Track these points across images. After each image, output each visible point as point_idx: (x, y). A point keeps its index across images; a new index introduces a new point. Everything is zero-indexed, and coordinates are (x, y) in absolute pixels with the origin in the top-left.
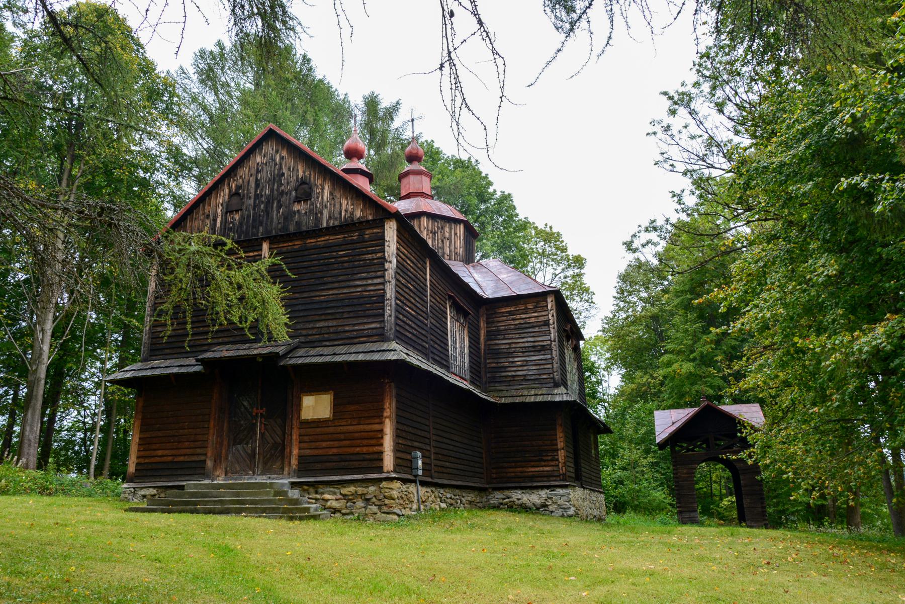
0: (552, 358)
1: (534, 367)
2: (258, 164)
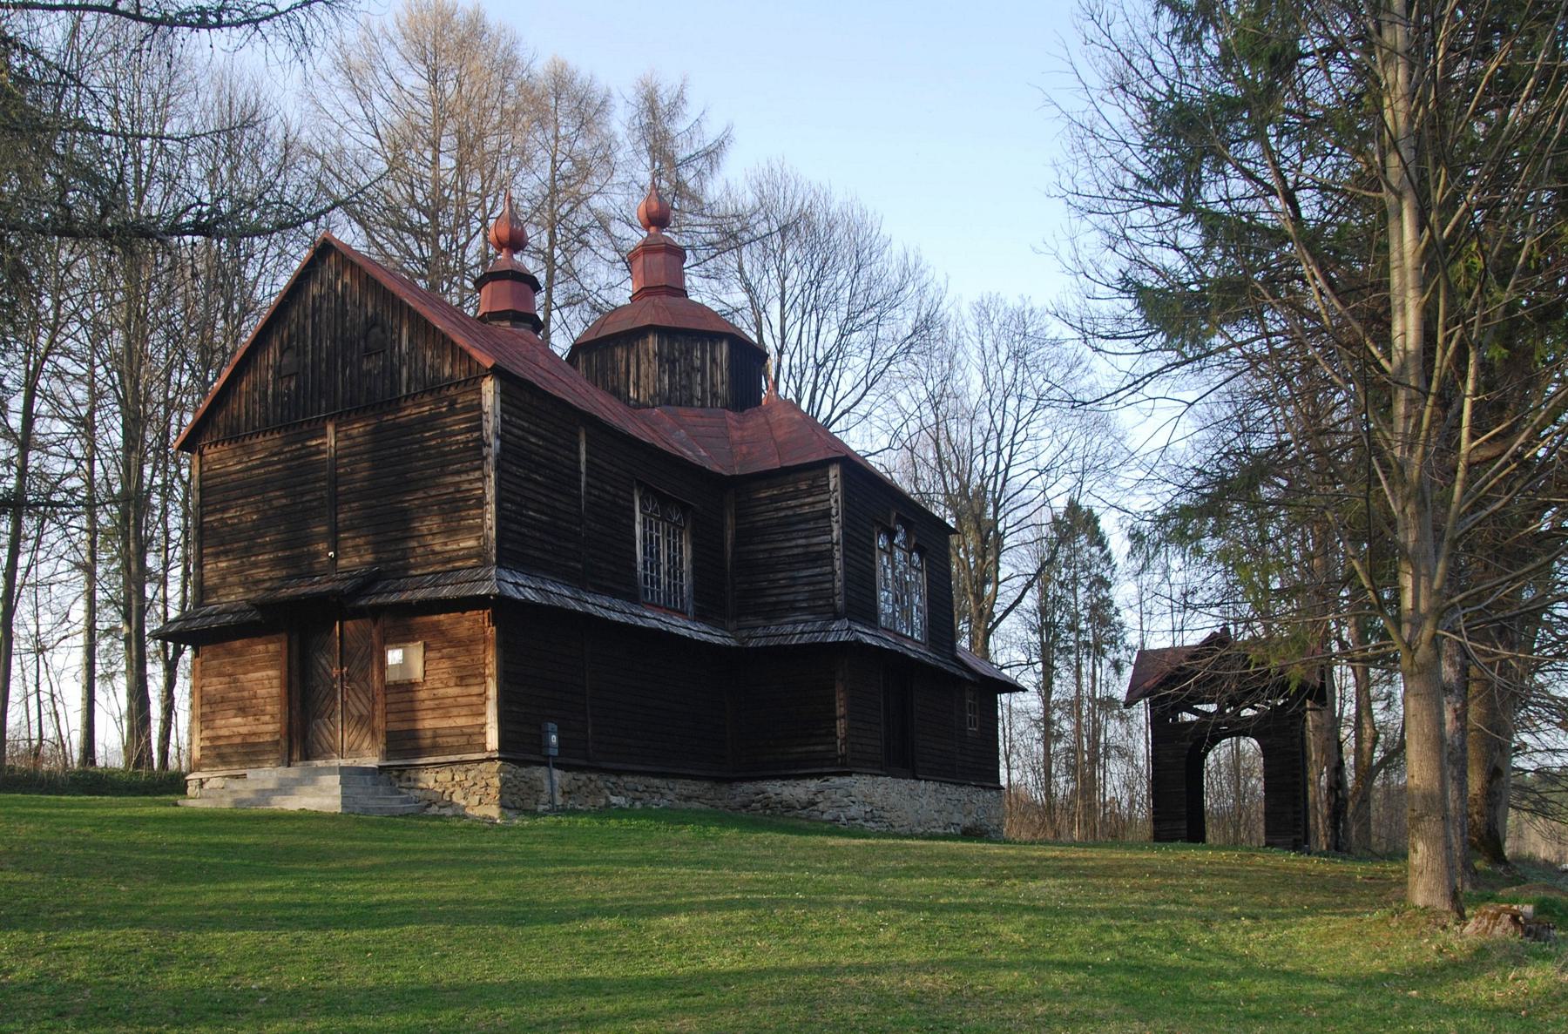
0: (833, 572)
1: (806, 588)
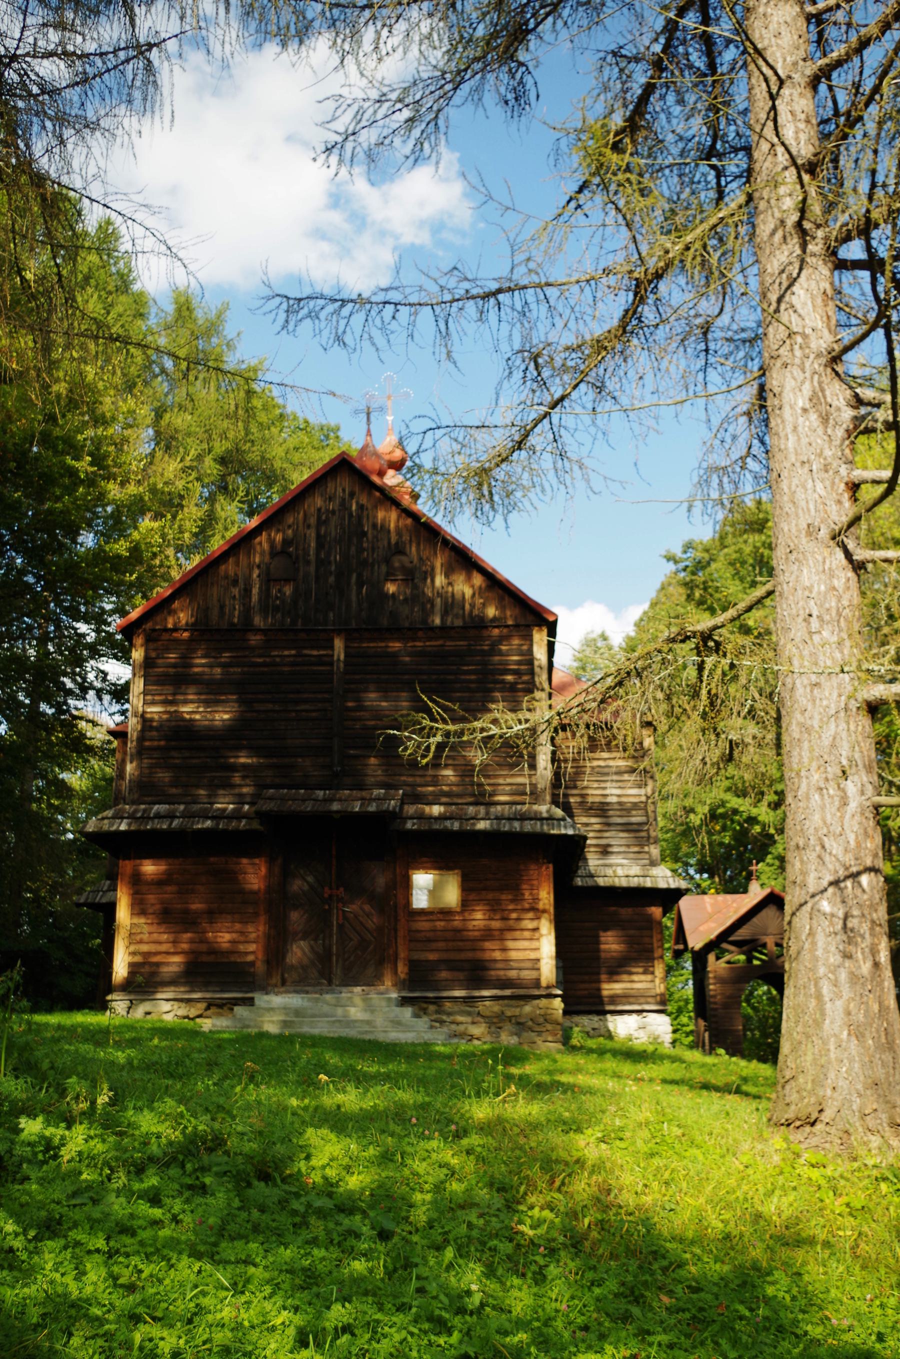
2: (319, 510)
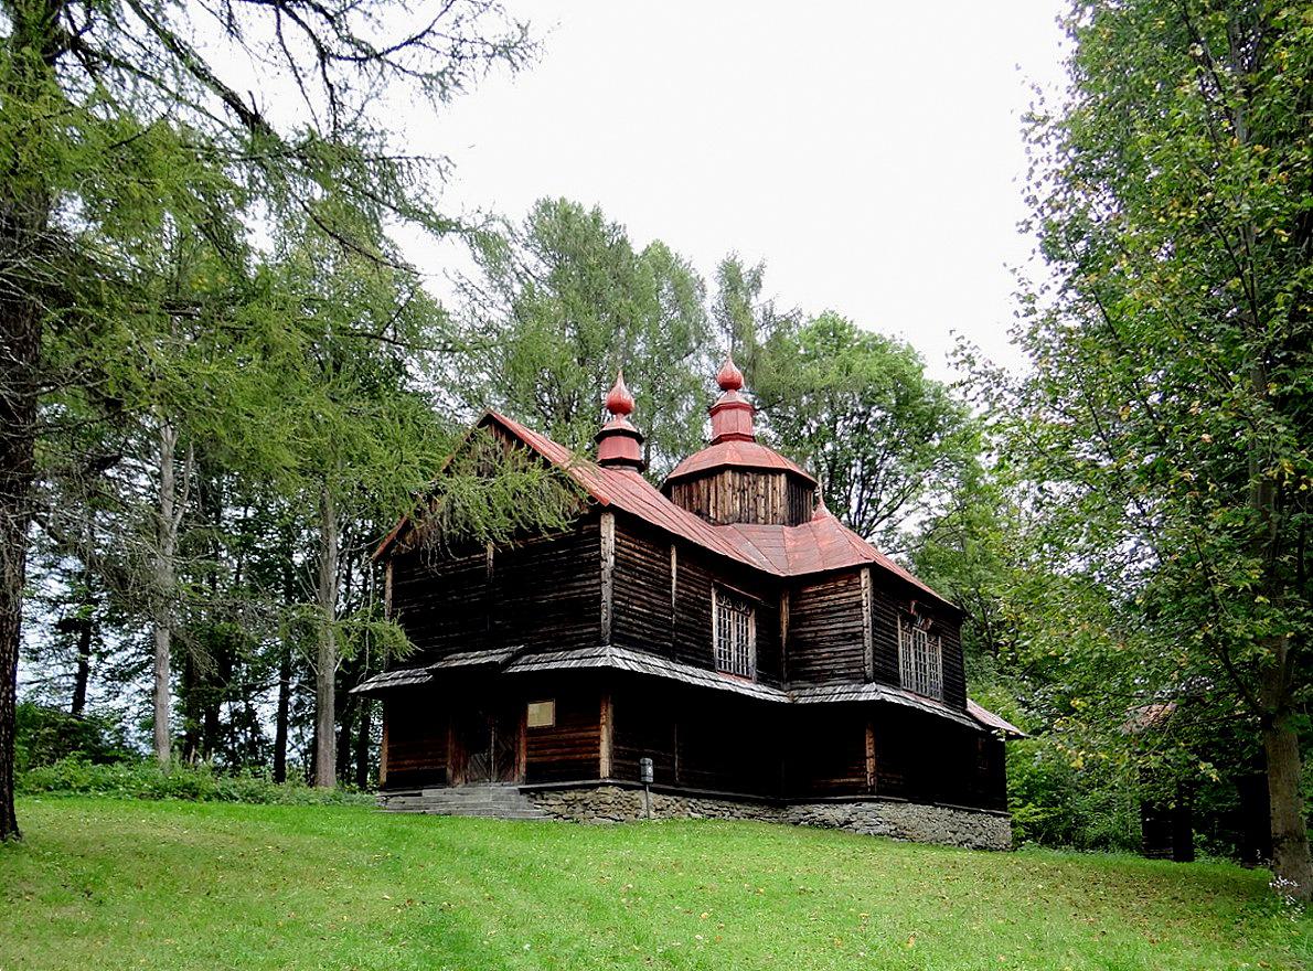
0: (864, 648)
